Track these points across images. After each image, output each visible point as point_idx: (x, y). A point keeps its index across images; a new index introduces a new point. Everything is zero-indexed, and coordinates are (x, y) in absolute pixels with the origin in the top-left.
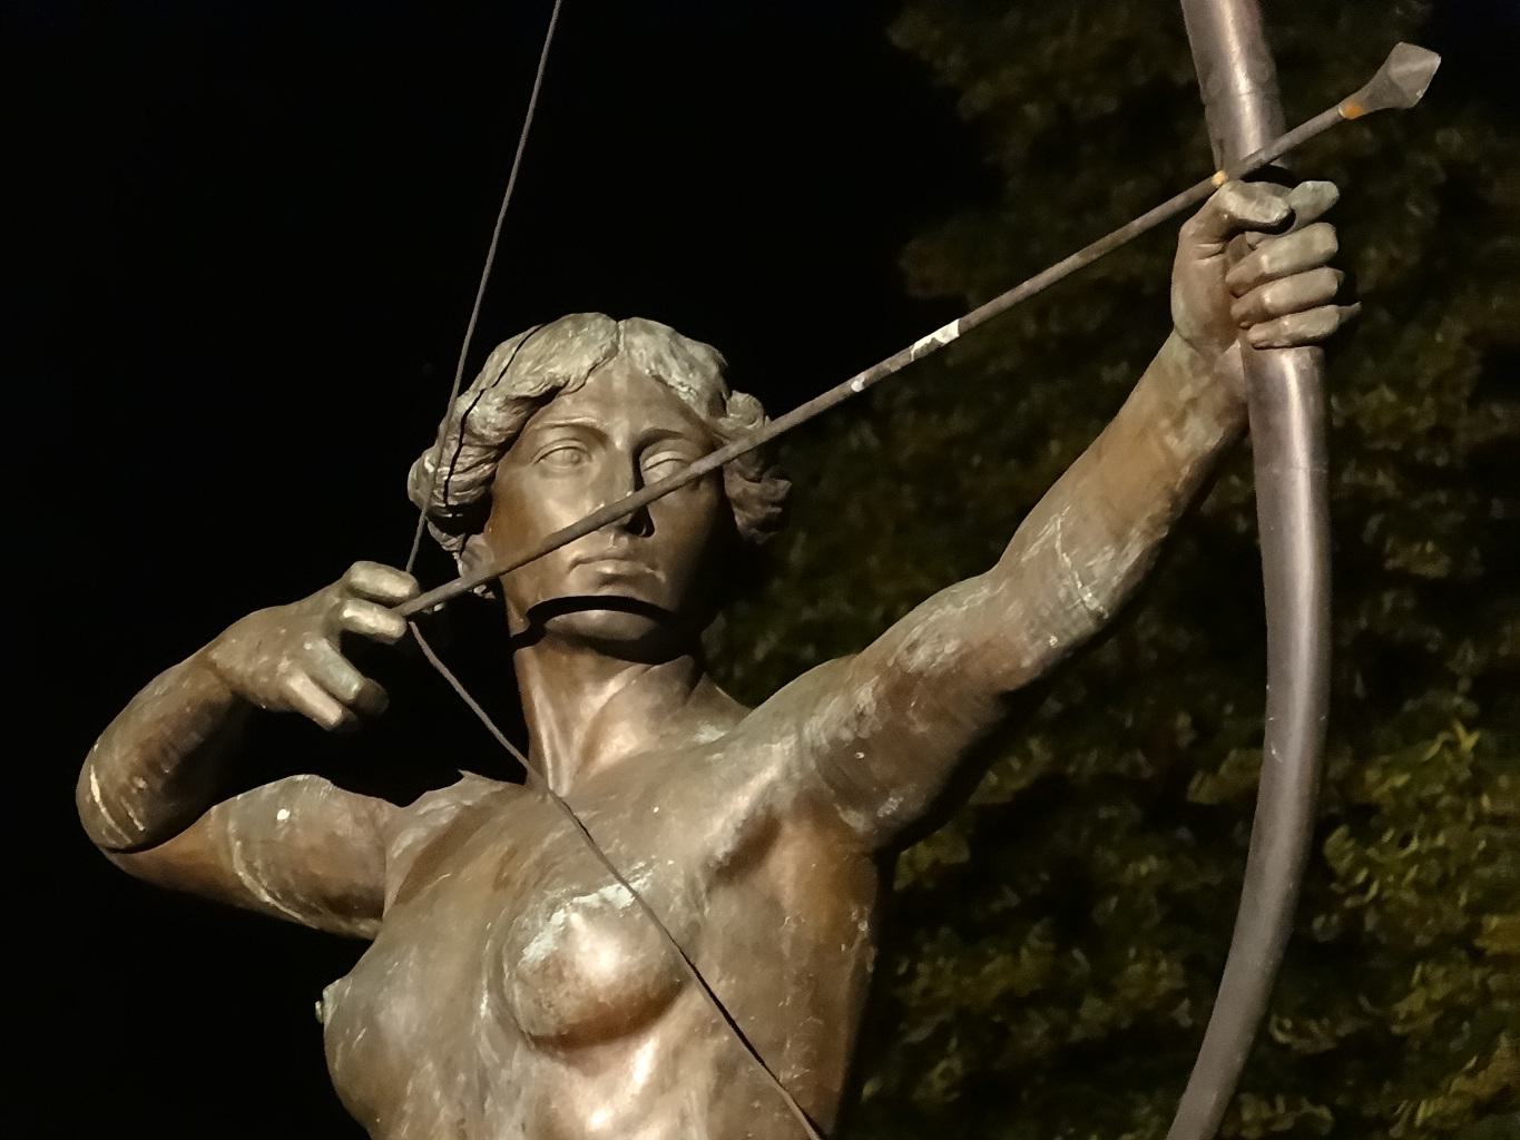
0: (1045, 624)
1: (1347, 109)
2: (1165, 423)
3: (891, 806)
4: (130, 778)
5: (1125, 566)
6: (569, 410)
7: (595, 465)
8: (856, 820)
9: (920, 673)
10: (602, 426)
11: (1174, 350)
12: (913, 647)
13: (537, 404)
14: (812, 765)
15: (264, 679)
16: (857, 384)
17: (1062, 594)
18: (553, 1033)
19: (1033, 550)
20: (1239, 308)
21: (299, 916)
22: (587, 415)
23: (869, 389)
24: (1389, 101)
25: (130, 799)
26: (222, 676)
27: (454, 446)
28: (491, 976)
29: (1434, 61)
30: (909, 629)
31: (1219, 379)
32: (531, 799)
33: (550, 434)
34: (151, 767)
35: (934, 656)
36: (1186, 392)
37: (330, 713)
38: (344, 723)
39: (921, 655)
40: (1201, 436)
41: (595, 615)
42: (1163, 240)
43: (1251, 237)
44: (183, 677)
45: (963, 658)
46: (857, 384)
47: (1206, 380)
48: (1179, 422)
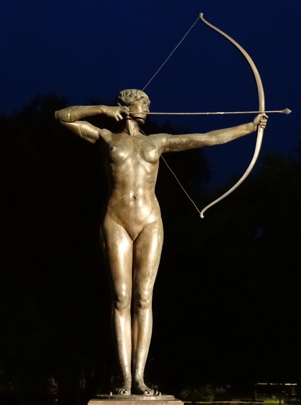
0: (219, 142)
1: (281, 111)
2: (246, 130)
3: (175, 150)
4: (77, 116)
5: (232, 140)
6: (144, 99)
7: (144, 105)
8: (168, 150)
9: (197, 141)
10: (146, 102)
11: (251, 124)
12: (197, 138)
13: (143, 97)
14: (168, 143)
15: (111, 114)
16: (208, 113)
17: (223, 140)
18: (150, 161)
19: (221, 135)
20: (261, 124)
21: (81, 135)
22: (145, 100)
23: (209, 114)
24: (285, 113)
25: (74, 118)
26: (102, 111)
27: (134, 98)
28: (140, 153)
29: (291, 111)
30: (195, 136)
31: (254, 128)
32: (124, 135)
33: (141, 101)
34: (82, 116)
35: (200, 140)
36: (250, 128)
37: (118, 120)
38: (118, 122)
39: (197, 139)
40: (248, 132)
41: (142, 120)
42: (256, 115)
43: (264, 118)
44: (93, 108)
45: (205, 142)
46: (208, 113)
47: (253, 128)
48: (247, 130)
